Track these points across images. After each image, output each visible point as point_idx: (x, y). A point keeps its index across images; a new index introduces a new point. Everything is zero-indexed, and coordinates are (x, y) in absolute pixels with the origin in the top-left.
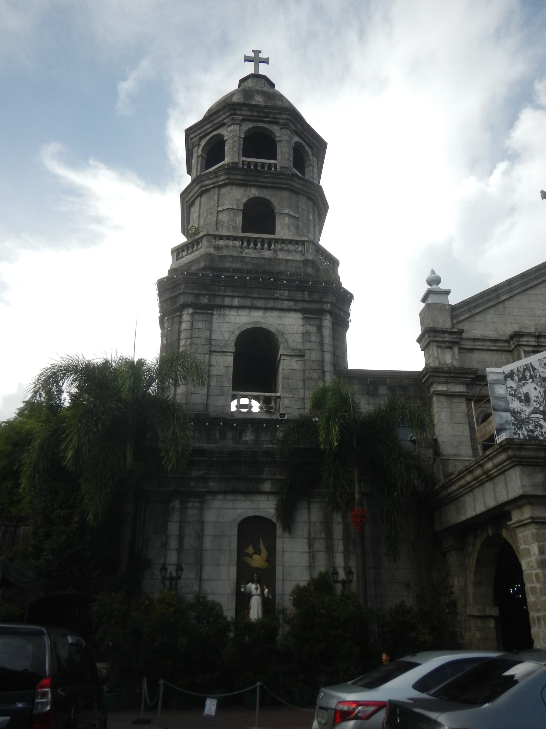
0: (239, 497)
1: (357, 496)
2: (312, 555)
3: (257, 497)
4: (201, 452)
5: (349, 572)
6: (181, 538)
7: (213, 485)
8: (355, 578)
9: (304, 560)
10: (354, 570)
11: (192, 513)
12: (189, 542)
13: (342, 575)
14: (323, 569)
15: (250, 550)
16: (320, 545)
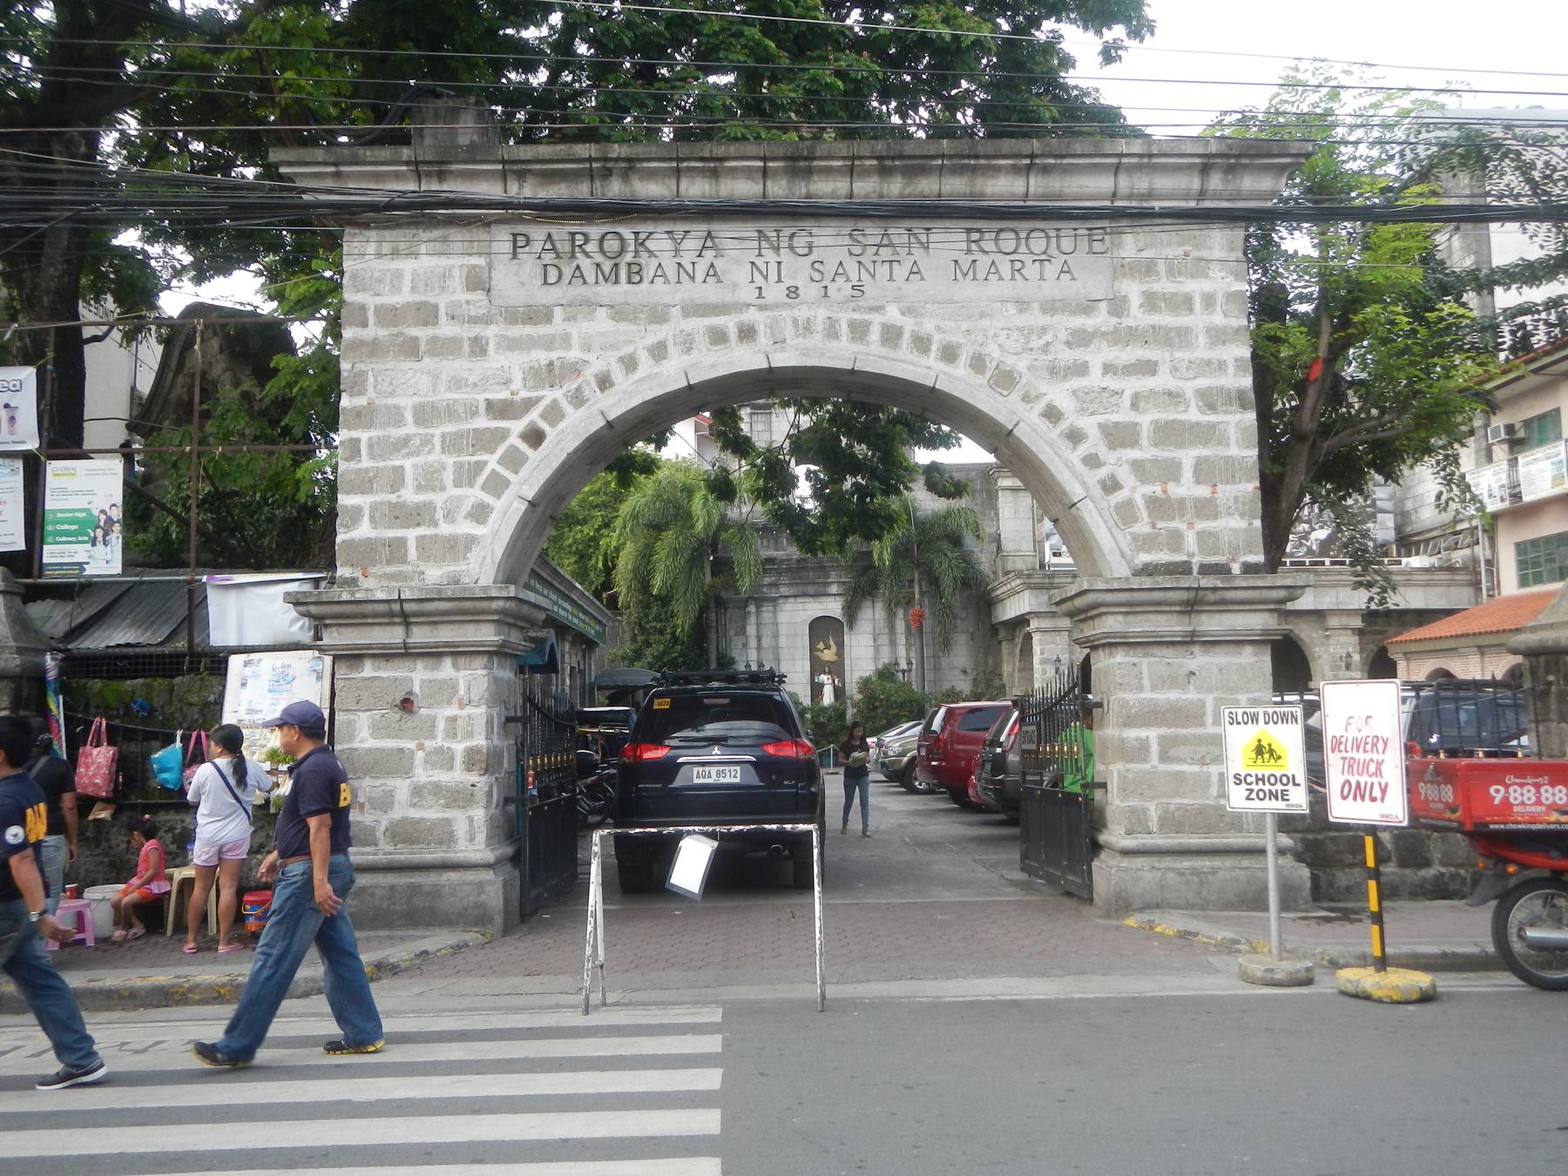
0: (808, 600)
1: (917, 596)
2: (877, 648)
3: (825, 599)
4: (771, 560)
5: (909, 663)
6: (759, 638)
7: (784, 590)
8: (914, 667)
9: (870, 652)
10: (914, 661)
11: (767, 615)
12: (766, 642)
13: (903, 665)
14: (886, 661)
15: (821, 646)
16: (884, 640)
